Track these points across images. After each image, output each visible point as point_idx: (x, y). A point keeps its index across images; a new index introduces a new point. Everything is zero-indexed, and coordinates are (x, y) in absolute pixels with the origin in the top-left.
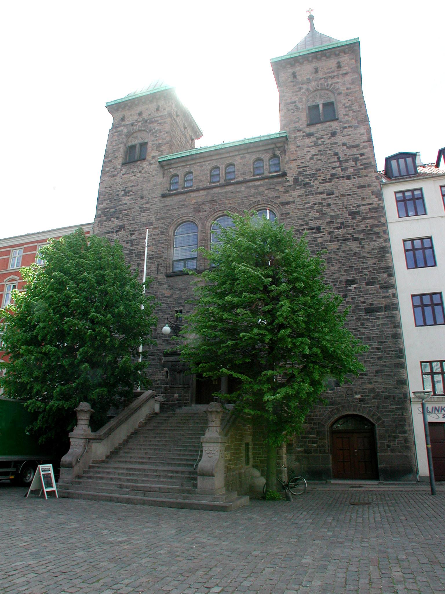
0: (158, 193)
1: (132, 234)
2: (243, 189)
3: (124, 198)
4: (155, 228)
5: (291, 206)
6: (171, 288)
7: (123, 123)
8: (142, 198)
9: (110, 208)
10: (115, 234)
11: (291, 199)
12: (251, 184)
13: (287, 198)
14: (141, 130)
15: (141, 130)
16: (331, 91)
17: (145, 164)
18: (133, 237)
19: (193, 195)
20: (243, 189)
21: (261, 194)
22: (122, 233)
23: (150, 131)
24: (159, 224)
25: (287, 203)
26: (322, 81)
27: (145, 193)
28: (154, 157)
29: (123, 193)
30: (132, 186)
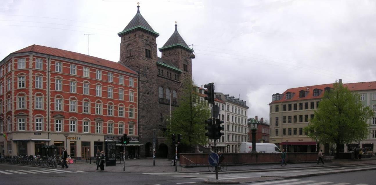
0: (156, 74)
1: (151, 85)
2: (173, 82)
3: (147, 70)
4: (156, 86)
5: (180, 92)
6: (160, 106)
7: (143, 37)
8: (152, 73)
9: (144, 72)
10: (146, 83)
11: (180, 90)
12: (174, 82)
13: (180, 89)
14: (149, 45)
15: (149, 45)
16: (187, 62)
17: (152, 60)
18: (151, 86)
19: (164, 79)
20: (173, 82)
21: (176, 86)
22: (148, 83)
23: (152, 47)
24: (157, 84)
25: (180, 91)
26: (186, 58)
27: (153, 72)
28: (154, 59)
29: (147, 68)
30: (149, 67)
